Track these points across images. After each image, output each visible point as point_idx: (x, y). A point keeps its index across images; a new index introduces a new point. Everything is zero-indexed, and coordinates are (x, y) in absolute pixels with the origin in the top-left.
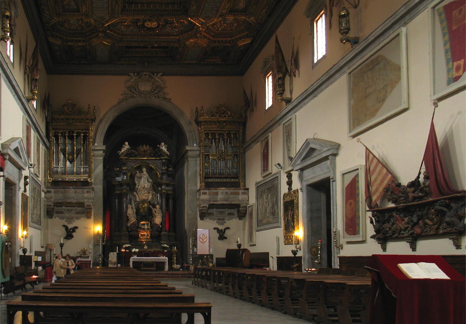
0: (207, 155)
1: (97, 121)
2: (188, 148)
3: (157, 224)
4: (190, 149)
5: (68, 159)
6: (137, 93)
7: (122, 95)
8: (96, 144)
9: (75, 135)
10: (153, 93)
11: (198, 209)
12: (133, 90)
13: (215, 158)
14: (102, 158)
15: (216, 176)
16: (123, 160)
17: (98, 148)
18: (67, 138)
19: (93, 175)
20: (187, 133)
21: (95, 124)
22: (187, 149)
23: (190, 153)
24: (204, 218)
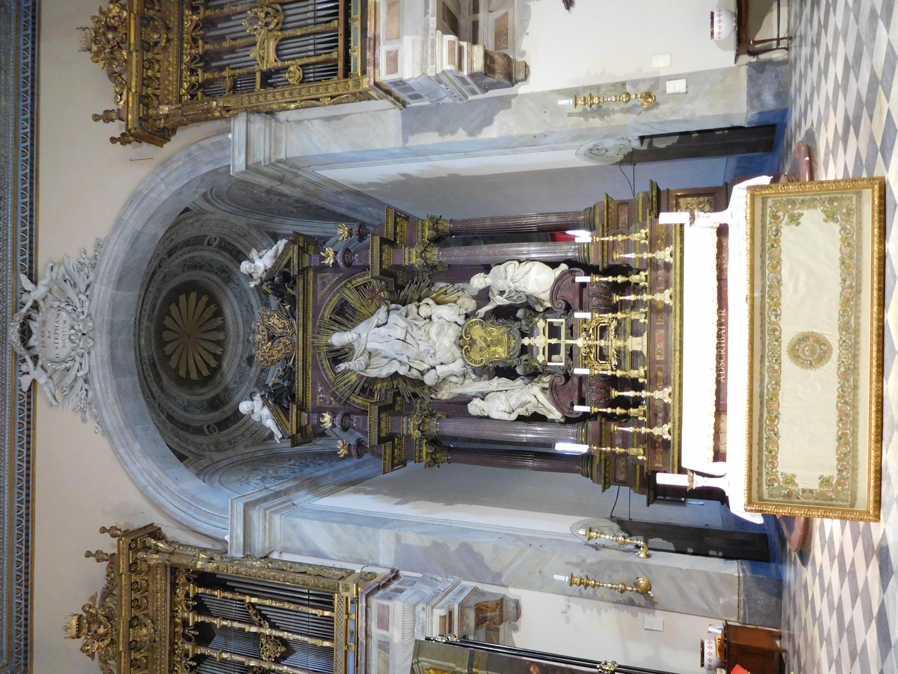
0: (265, 84)
1: (159, 521)
2: (238, 163)
3: (552, 281)
4: (243, 156)
5: (277, 661)
6: (77, 365)
7: (84, 420)
8: (227, 538)
9: (193, 618)
10: (78, 305)
11: (481, 96)
12: (68, 380)
13: (272, 45)
14: (277, 518)
15: (341, 31)
16: (304, 422)
17: (240, 531)
18: (200, 651)
19: (338, 565)
20: (198, 174)
21: (170, 531)
22: (243, 168)
23: (261, 154)
24: (519, 59)
